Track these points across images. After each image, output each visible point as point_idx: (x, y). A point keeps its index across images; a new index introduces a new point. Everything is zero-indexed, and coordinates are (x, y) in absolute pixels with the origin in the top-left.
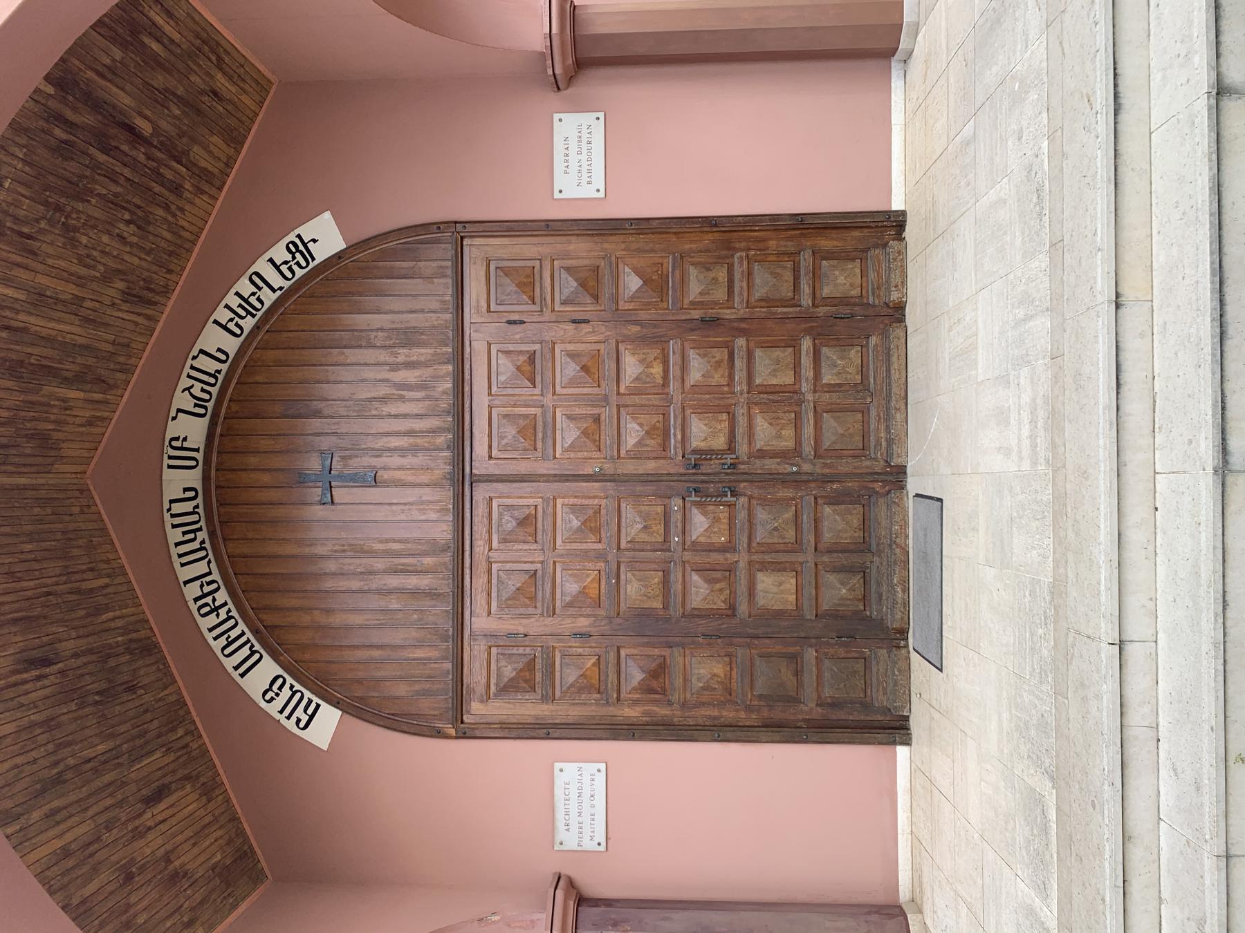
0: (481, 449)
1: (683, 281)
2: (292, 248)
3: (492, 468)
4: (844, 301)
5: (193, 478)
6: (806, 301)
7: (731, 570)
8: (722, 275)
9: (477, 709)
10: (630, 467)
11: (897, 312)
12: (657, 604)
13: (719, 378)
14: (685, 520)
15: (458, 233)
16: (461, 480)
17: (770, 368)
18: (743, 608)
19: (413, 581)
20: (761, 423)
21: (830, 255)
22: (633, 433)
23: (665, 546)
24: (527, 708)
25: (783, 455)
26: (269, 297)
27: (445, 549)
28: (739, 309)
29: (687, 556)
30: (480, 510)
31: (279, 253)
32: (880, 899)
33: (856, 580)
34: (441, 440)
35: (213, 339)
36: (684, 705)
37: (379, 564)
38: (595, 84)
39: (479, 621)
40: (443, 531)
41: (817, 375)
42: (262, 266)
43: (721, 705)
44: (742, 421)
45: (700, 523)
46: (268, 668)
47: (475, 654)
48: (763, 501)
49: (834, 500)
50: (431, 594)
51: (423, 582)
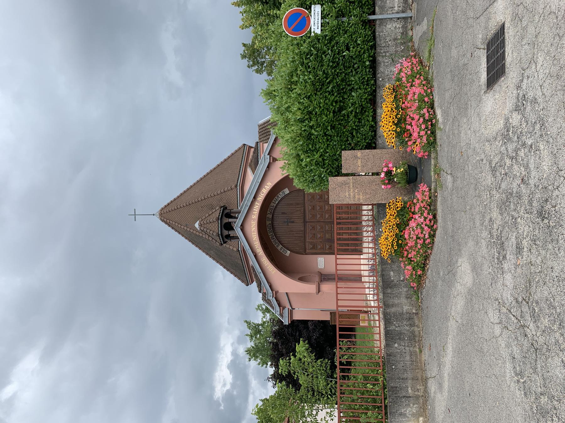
5: (270, 222)
16: (305, 222)
22: (327, 216)
24: (314, 251)
31: (281, 193)
35: (272, 204)
39: (307, 240)
40: (303, 229)
46: (281, 246)
47: (307, 244)
50: (301, 237)
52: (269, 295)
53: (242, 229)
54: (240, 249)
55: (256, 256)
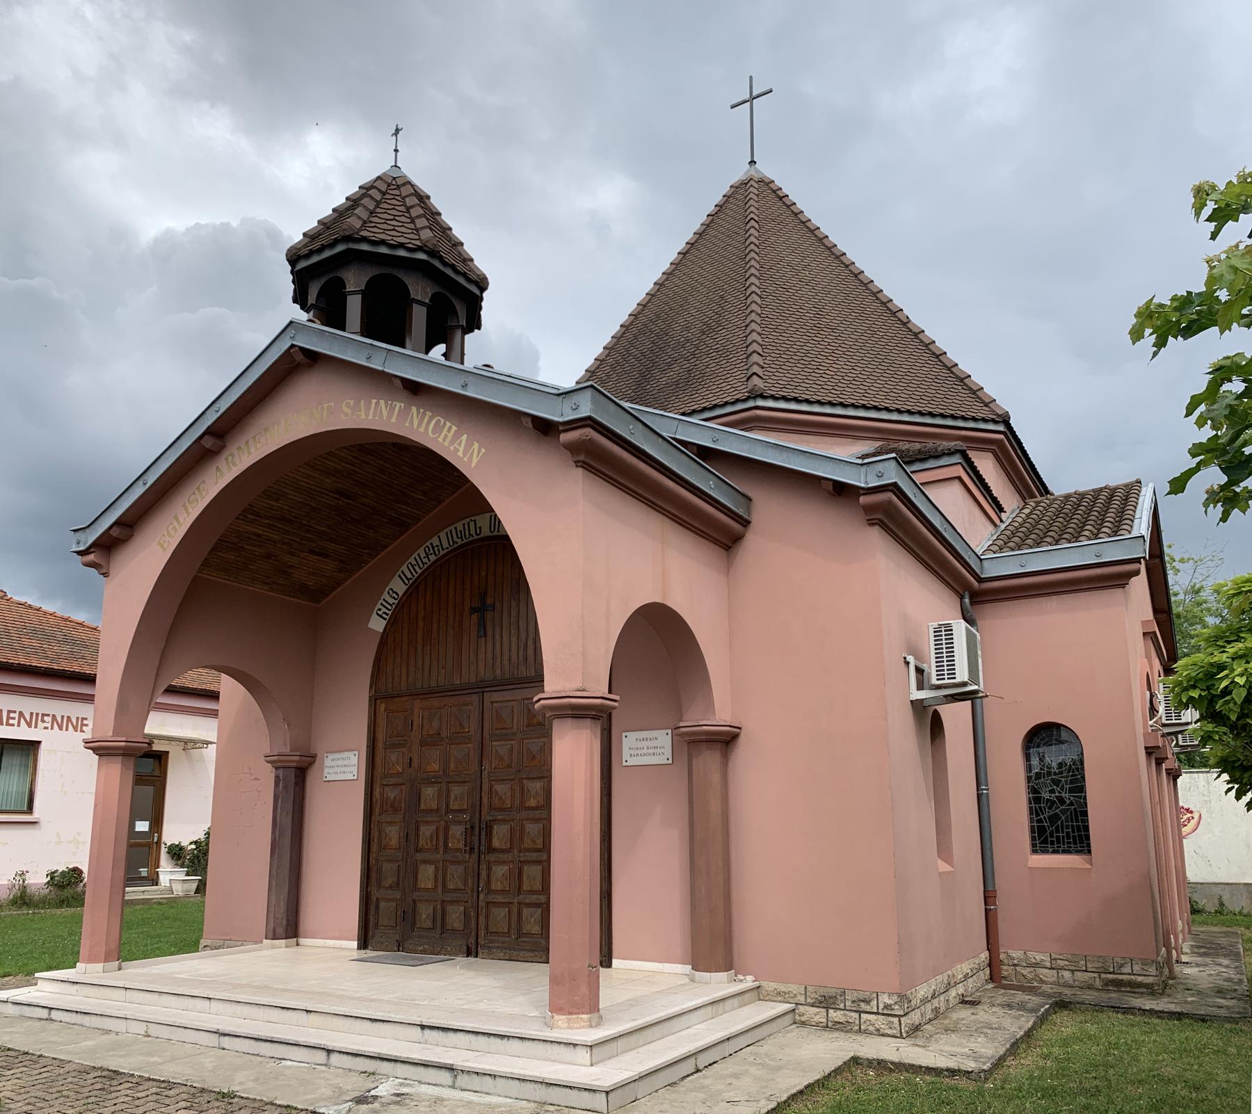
12: (423, 807)
13: (527, 843)
14: (460, 823)
18: (419, 856)
20: (505, 868)
23: (448, 811)
29: (443, 823)
32: (302, 928)
41: (529, 905)
43: (380, 843)
45: (457, 831)
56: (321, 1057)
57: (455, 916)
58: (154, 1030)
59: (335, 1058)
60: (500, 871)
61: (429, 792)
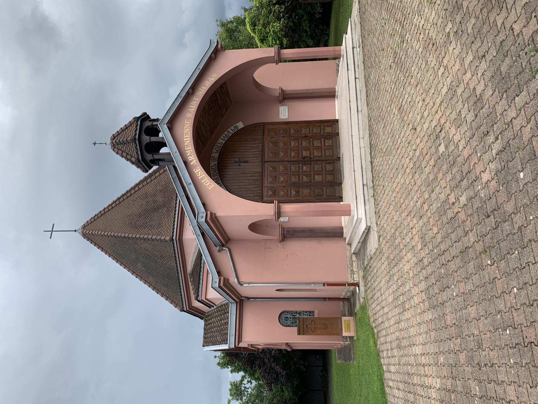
0: (266, 157)
1: (301, 130)
2: (235, 127)
3: (268, 160)
4: (329, 133)
5: (216, 163)
6: (322, 133)
7: (310, 175)
8: (308, 129)
9: (265, 199)
10: (292, 159)
11: (338, 134)
14: (302, 167)
15: (264, 124)
16: (263, 162)
17: (316, 143)
19: (254, 178)
20: (315, 152)
21: (326, 126)
25: (319, 157)
26: (230, 135)
27: (260, 173)
28: (311, 134)
30: (266, 167)
31: (232, 128)
33: (332, 176)
34: (259, 156)
35: (220, 141)
36: (302, 197)
37: (248, 175)
38: (286, 102)
39: (266, 184)
40: (260, 170)
42: (229, 130)
44: (312, 152)
47: (265, 190)
48: (316, 164)
49: (328, 163)
50: (257, 180)
51: (256, 178)
52: (200, 215)
53: (170, 129)
54: (174, 238)
55: (186, 163)
56: (357, 80)
57: (329, 167)
58: (361, 136)
59: (357, 76)
60: (316, 153)
61: (294, 179)
